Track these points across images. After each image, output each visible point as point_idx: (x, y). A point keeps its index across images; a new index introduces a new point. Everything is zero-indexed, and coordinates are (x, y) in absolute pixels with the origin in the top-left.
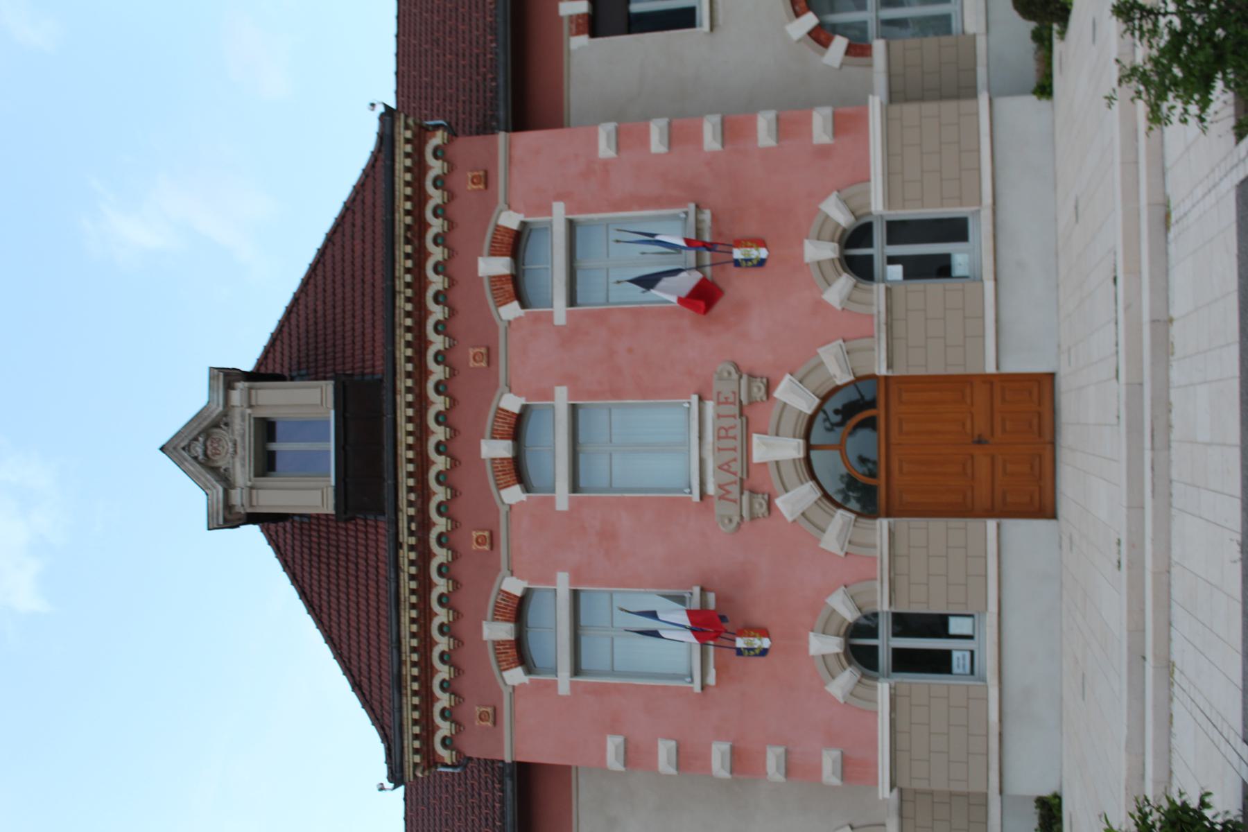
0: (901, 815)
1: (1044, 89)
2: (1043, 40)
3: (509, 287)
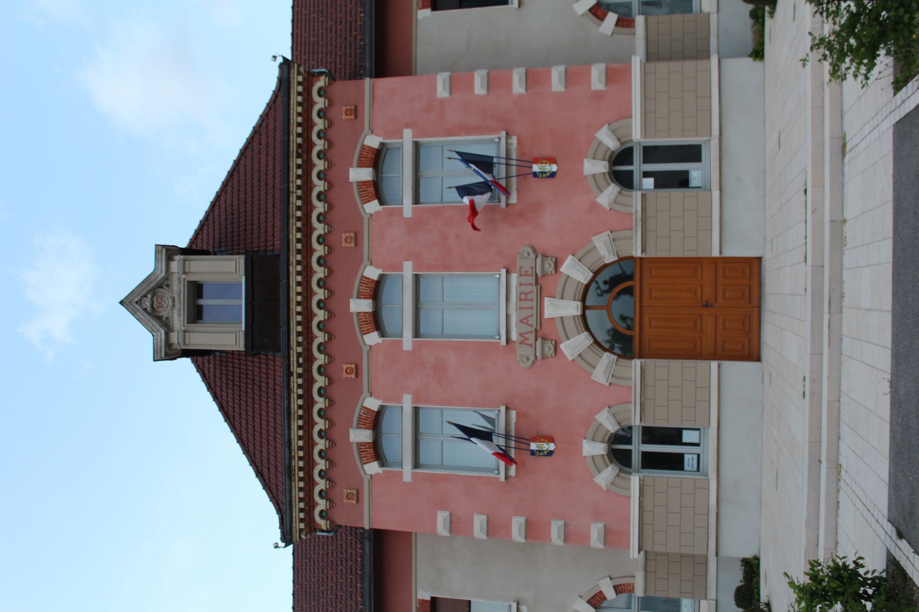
0: (646, 570)
1: (758, 53)
2: (758, 18)
3: (372, 190)
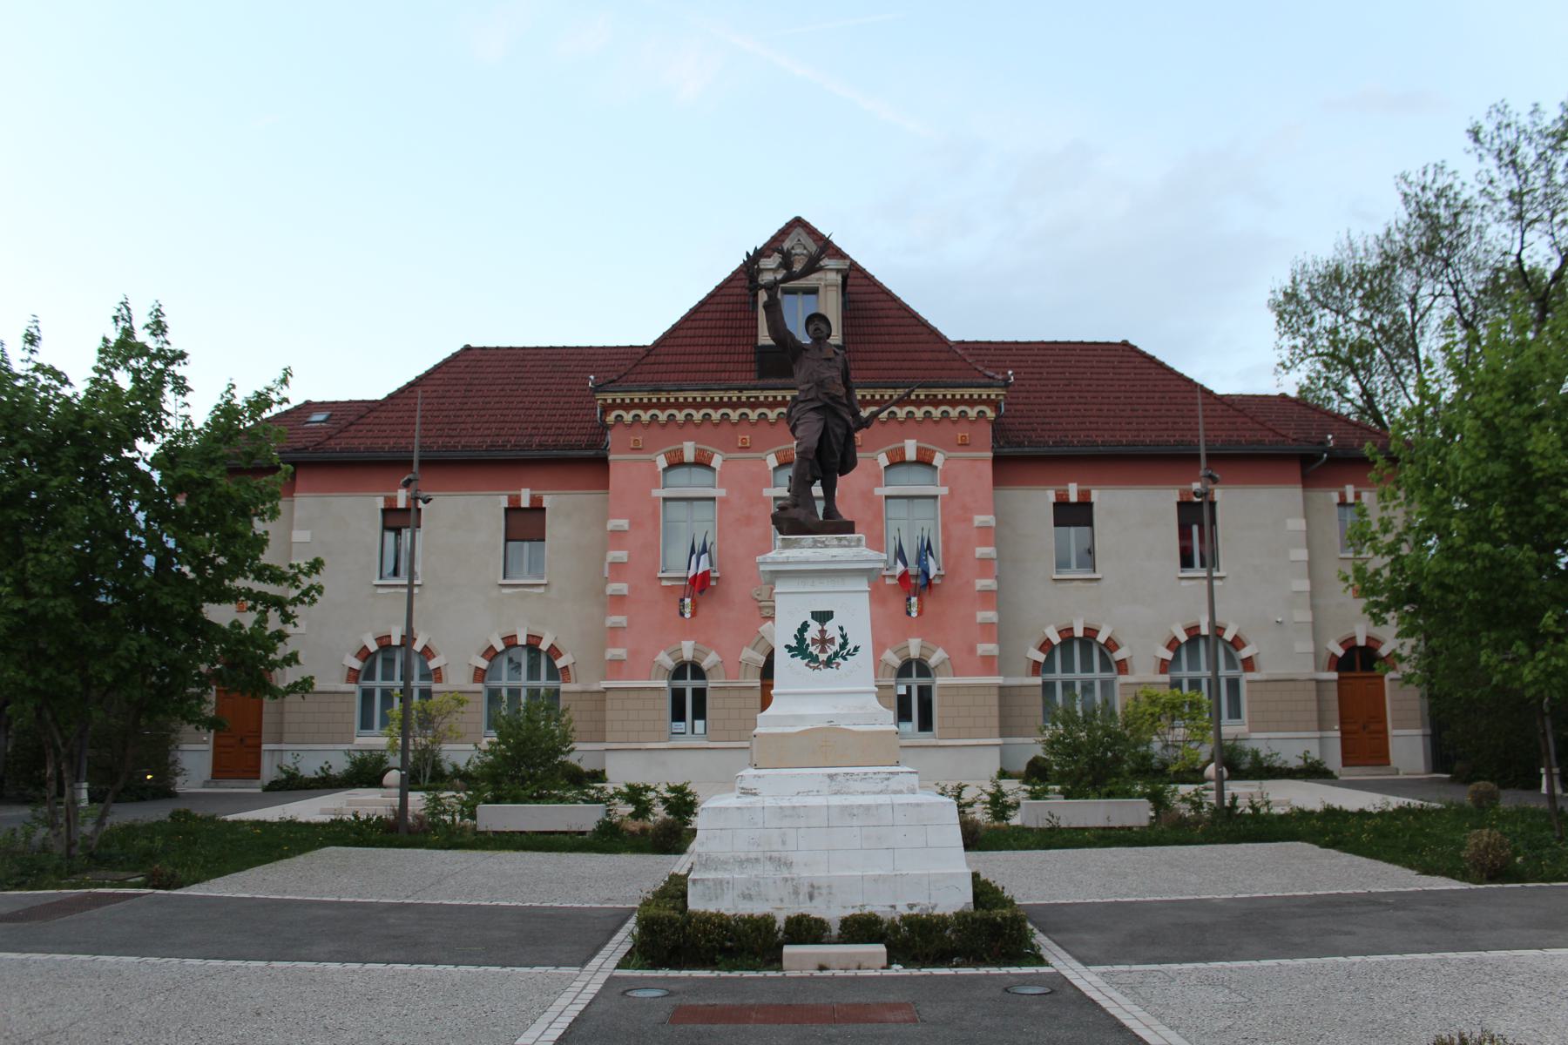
3: (898, 460)
